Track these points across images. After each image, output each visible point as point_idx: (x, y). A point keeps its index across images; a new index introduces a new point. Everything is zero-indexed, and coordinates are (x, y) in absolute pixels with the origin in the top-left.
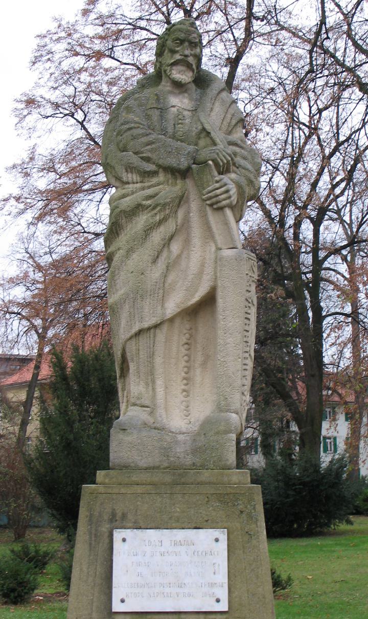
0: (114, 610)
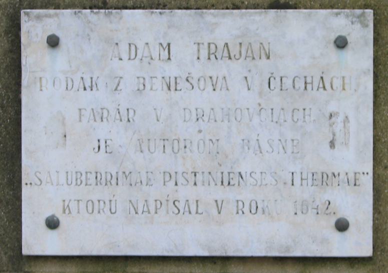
0: (25, 251)
